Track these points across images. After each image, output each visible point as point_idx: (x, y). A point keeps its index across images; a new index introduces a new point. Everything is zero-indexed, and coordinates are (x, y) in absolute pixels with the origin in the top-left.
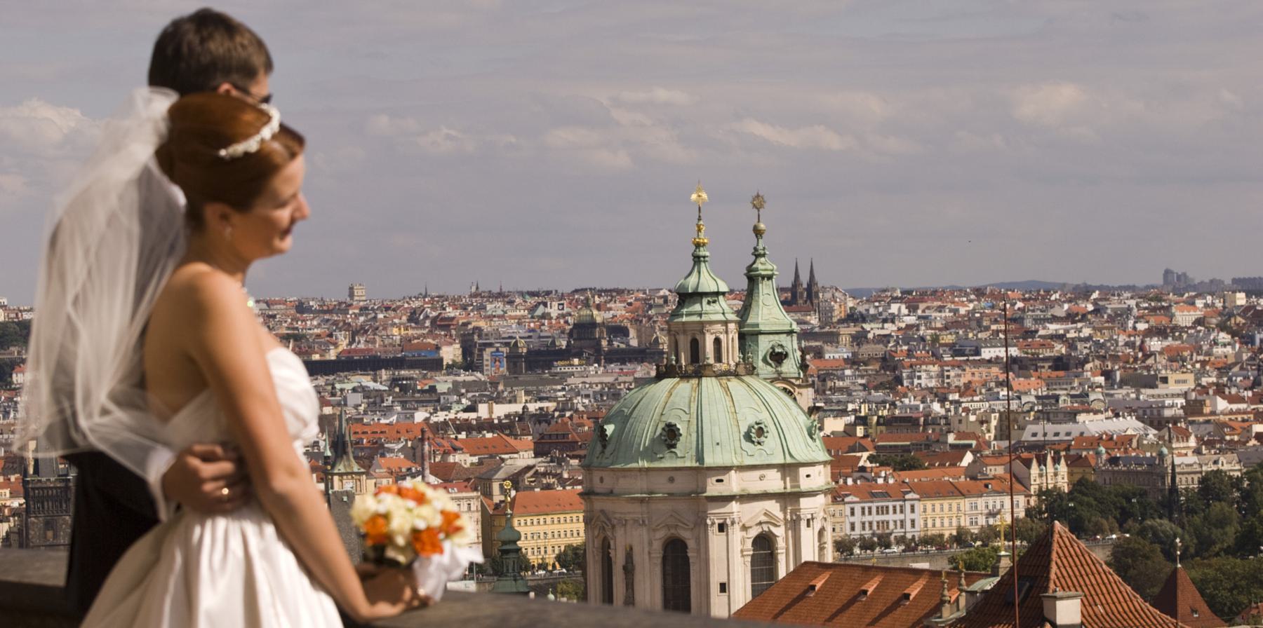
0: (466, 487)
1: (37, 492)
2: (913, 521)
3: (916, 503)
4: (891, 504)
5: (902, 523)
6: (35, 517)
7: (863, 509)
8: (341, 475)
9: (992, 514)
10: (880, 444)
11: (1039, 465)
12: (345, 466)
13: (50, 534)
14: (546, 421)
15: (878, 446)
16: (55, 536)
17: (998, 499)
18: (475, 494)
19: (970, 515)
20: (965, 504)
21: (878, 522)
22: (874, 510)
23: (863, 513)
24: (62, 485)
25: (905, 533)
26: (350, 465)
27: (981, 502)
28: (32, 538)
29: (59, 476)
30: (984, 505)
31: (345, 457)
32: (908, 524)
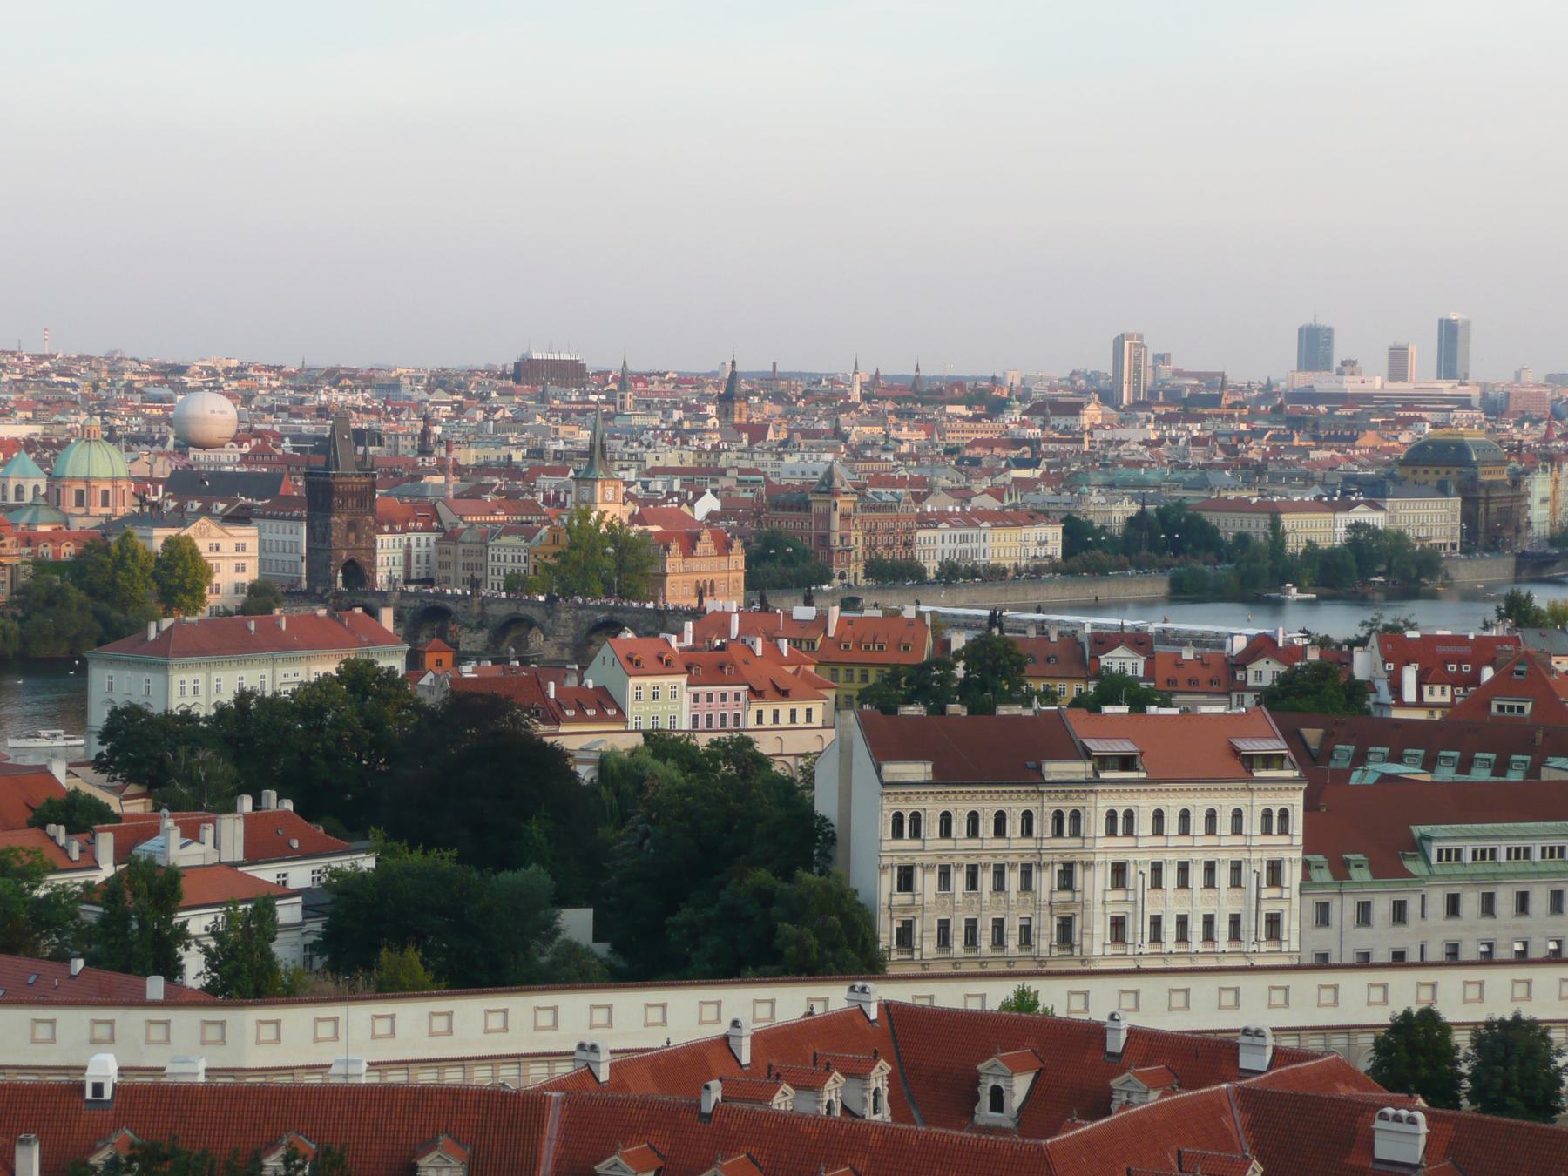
13: (352, 536)
16: (358, 539)
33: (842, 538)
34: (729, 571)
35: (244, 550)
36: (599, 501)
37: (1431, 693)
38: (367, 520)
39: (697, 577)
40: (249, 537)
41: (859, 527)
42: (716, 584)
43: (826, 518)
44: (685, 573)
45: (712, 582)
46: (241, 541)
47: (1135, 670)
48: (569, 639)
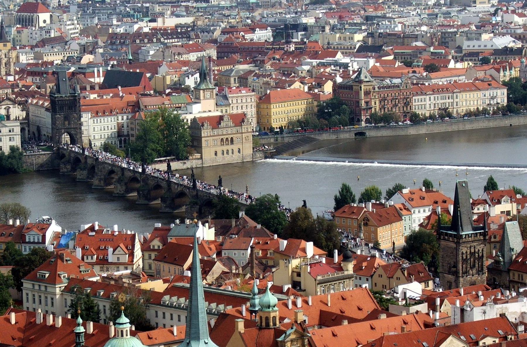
0: (249, 90)
1: (60, 102)
2: (457, 103)
3: (458, 94)
4: (447, 95)
5: (452, 103)
6: (59, 115)
7: (435, 97)
8: (204, 90)
9: (493, 98)
10: (395, 51)
11: (504, 71)
12: (205, 85)
13: (67, 123)
14: (207, 32)
15: (395, 52)
16: (69, 124)
17: (495, 91)
18: (253, 93)
19: (482, 99)
20: (480, 94)
21: (441, 104)
22: (439, 98)
23: (435, 99)
24: (72, 98)
25: (453, 108)
26: (208, 85)
27: (487, 93)
28: (58, 125)
29: (70, 94)
30: (489, 94)
31: (205, 80)
32: (455, 104)
33: (367, 103)
34: (242, 133)
35: (13, 131)
36: (202, 98)
37: (87, 258)
38: (73, 115)
39: (222, 137)
40: (16, 126)
41: (377, 97)
42: (234, 139)
43: (358, 93)
44: (214, 136)
45: (232, 138)
46: (11, 128)
47: (38, 239)
48: (102, 177)
